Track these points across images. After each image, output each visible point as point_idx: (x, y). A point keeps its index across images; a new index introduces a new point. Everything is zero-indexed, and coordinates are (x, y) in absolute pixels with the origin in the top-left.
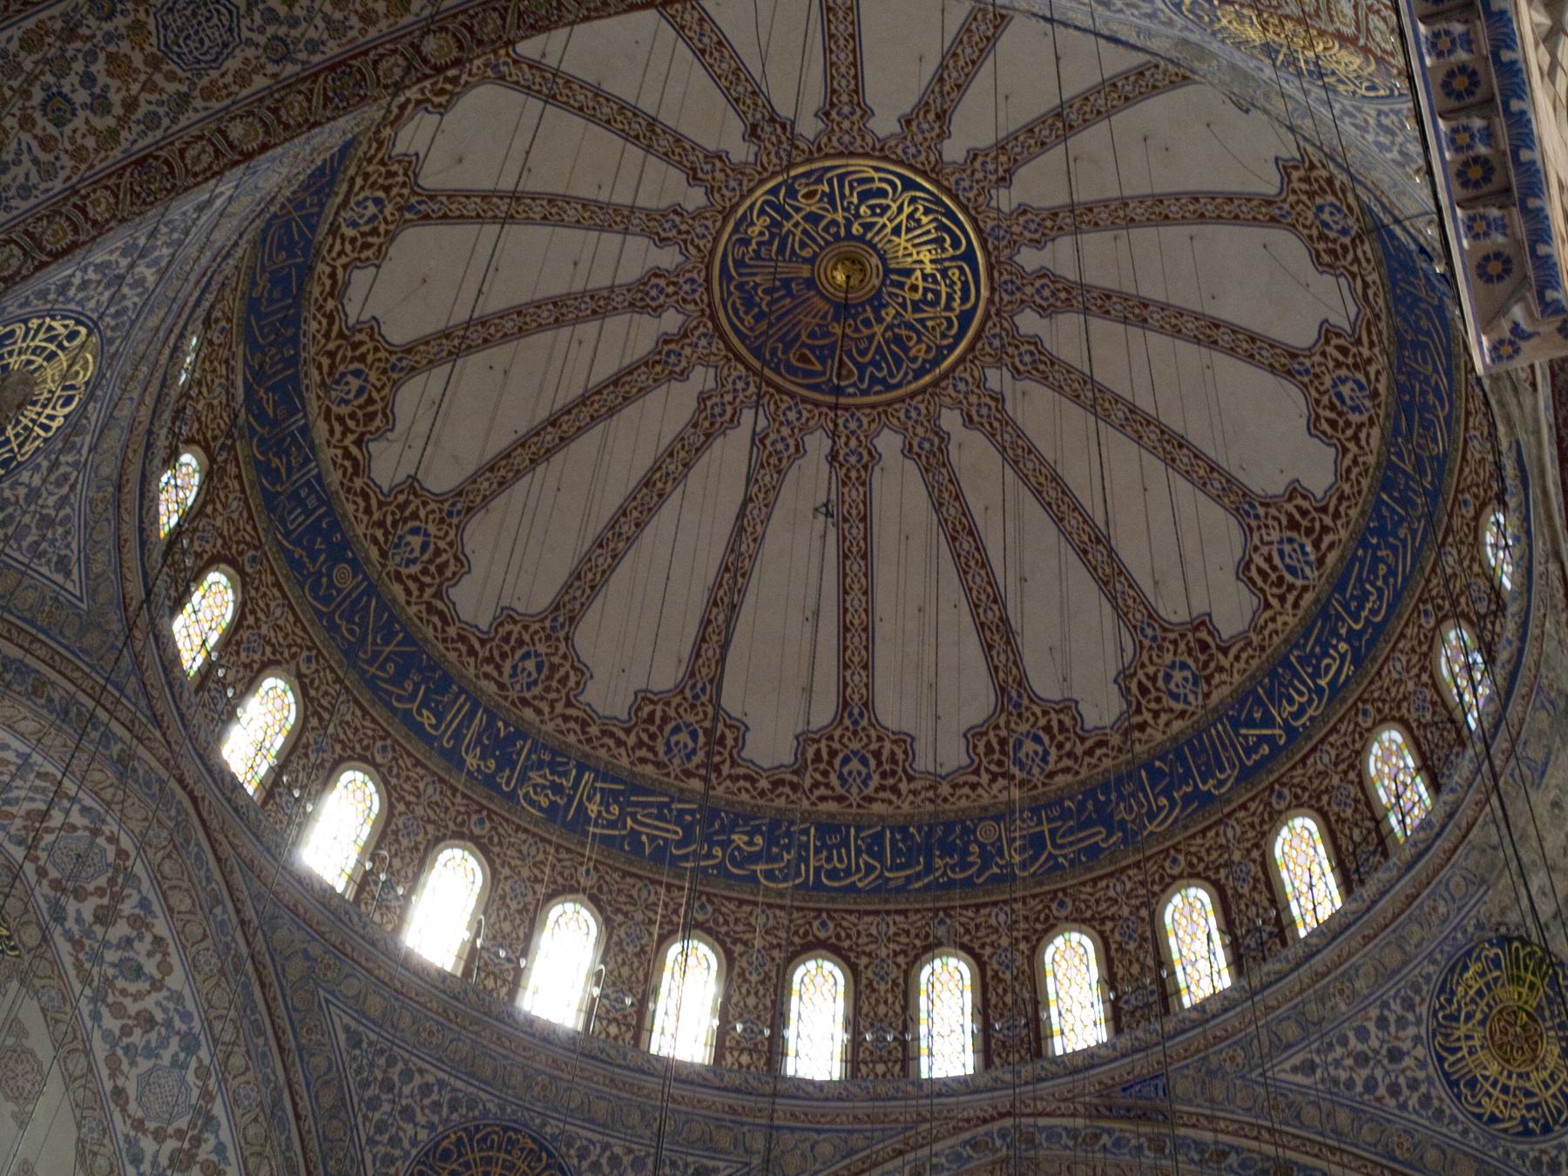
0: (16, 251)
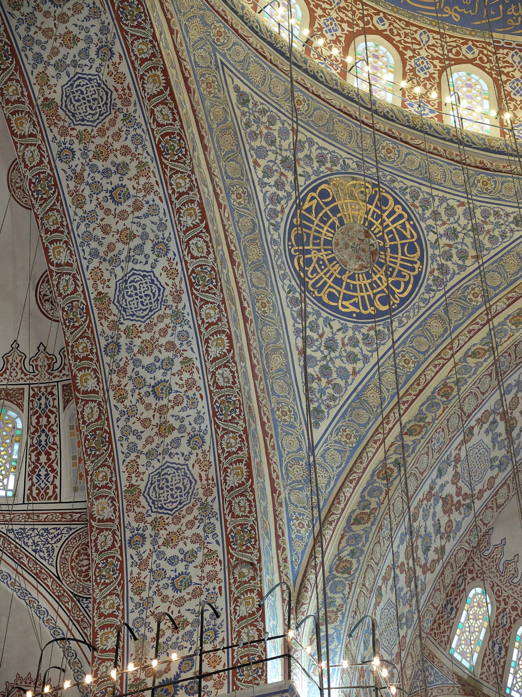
0: (194, 241)
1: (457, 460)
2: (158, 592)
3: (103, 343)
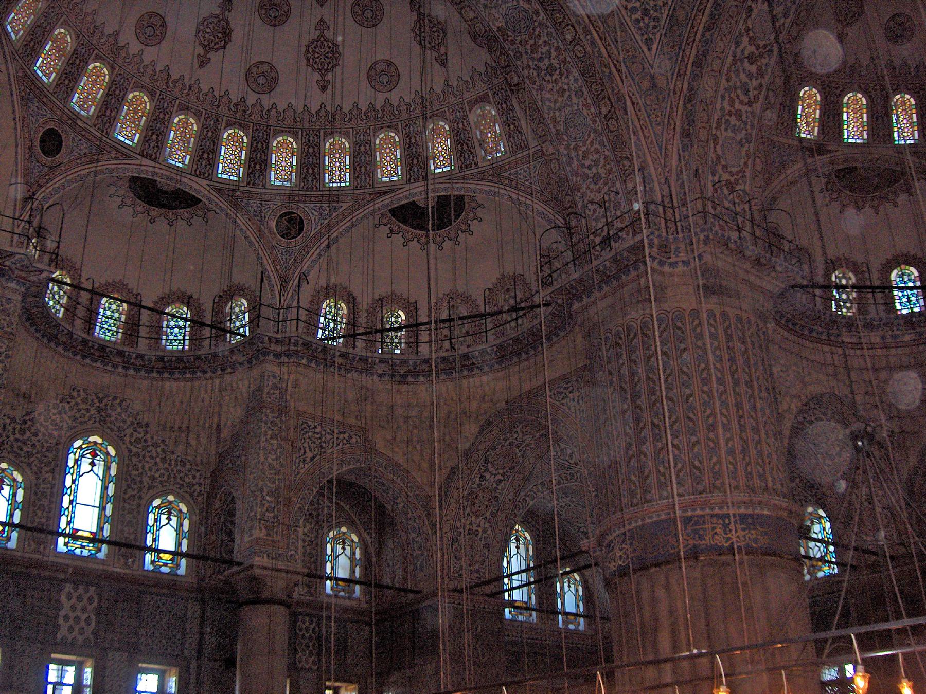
1: (748, 30)
2: (588, 188)
3: (512, 54)
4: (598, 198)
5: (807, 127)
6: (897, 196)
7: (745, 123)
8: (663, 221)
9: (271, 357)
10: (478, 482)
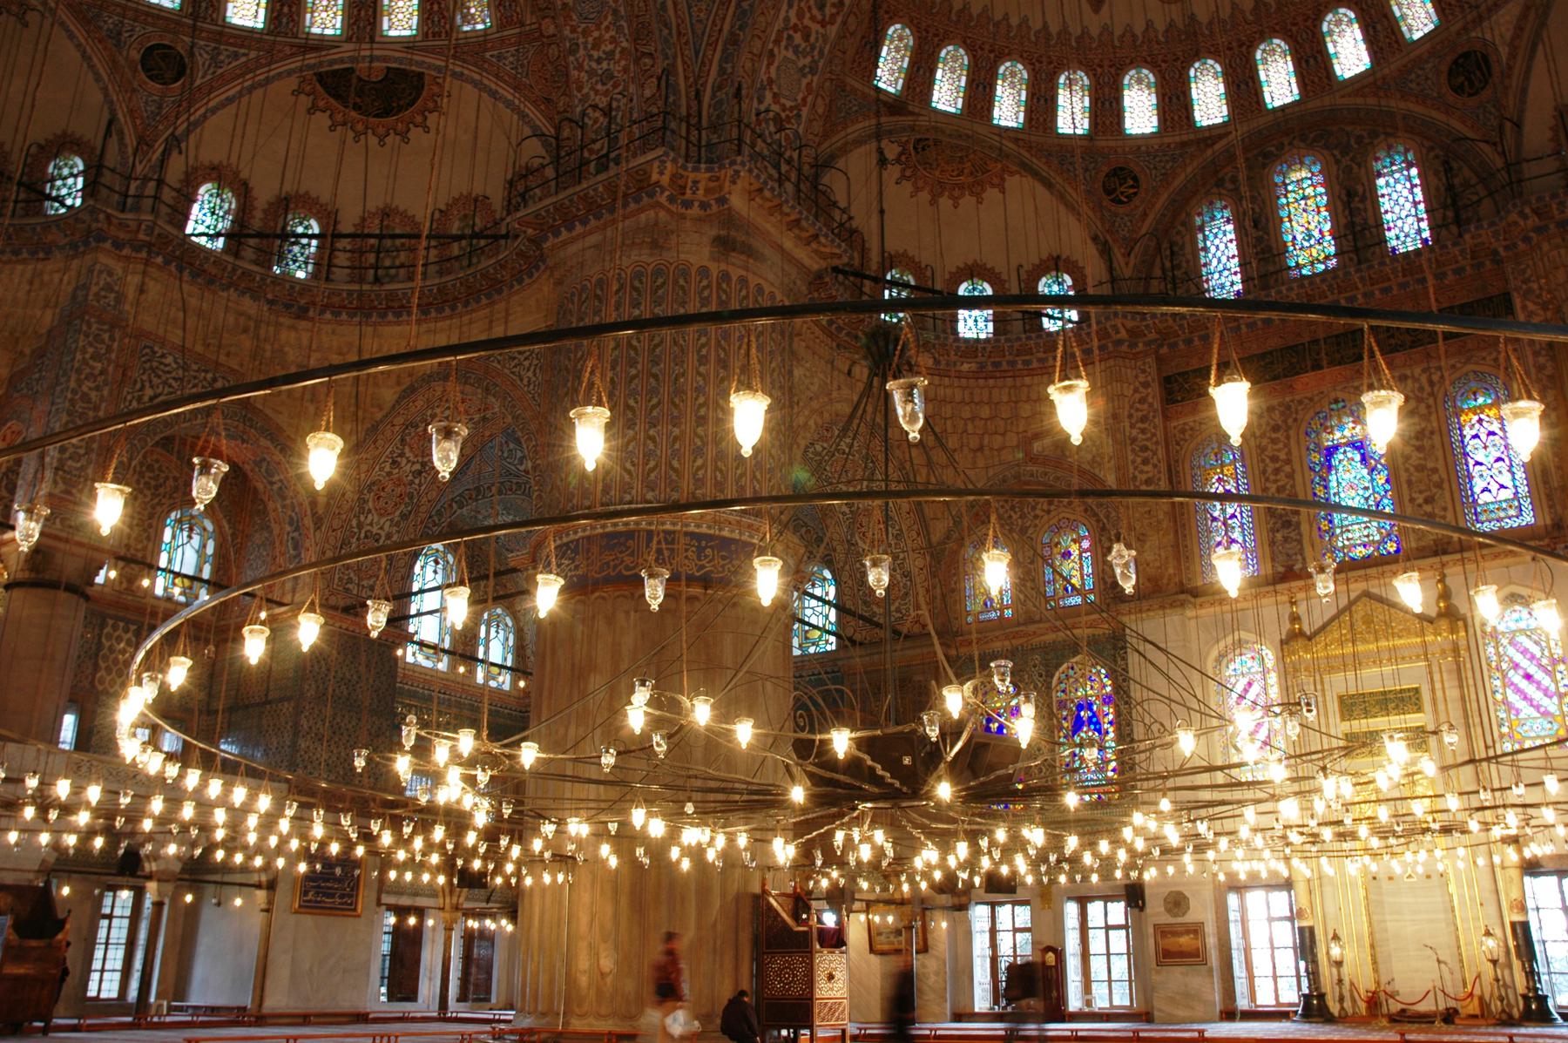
4: (603, 102)
5: (889, 75)
6: (983, 190)
7: (813, 48)
8: (684, 142)
9: (108, 245)
10: (387, 469)
